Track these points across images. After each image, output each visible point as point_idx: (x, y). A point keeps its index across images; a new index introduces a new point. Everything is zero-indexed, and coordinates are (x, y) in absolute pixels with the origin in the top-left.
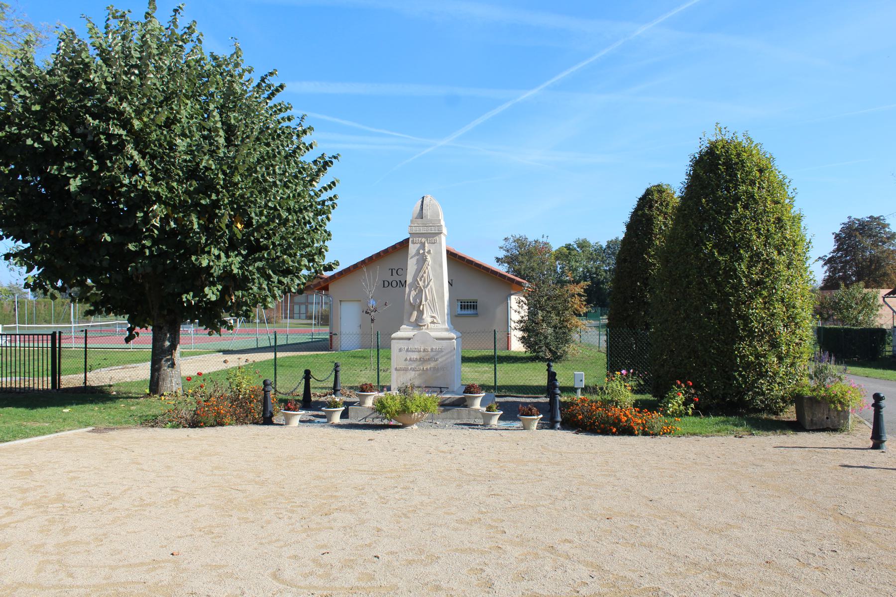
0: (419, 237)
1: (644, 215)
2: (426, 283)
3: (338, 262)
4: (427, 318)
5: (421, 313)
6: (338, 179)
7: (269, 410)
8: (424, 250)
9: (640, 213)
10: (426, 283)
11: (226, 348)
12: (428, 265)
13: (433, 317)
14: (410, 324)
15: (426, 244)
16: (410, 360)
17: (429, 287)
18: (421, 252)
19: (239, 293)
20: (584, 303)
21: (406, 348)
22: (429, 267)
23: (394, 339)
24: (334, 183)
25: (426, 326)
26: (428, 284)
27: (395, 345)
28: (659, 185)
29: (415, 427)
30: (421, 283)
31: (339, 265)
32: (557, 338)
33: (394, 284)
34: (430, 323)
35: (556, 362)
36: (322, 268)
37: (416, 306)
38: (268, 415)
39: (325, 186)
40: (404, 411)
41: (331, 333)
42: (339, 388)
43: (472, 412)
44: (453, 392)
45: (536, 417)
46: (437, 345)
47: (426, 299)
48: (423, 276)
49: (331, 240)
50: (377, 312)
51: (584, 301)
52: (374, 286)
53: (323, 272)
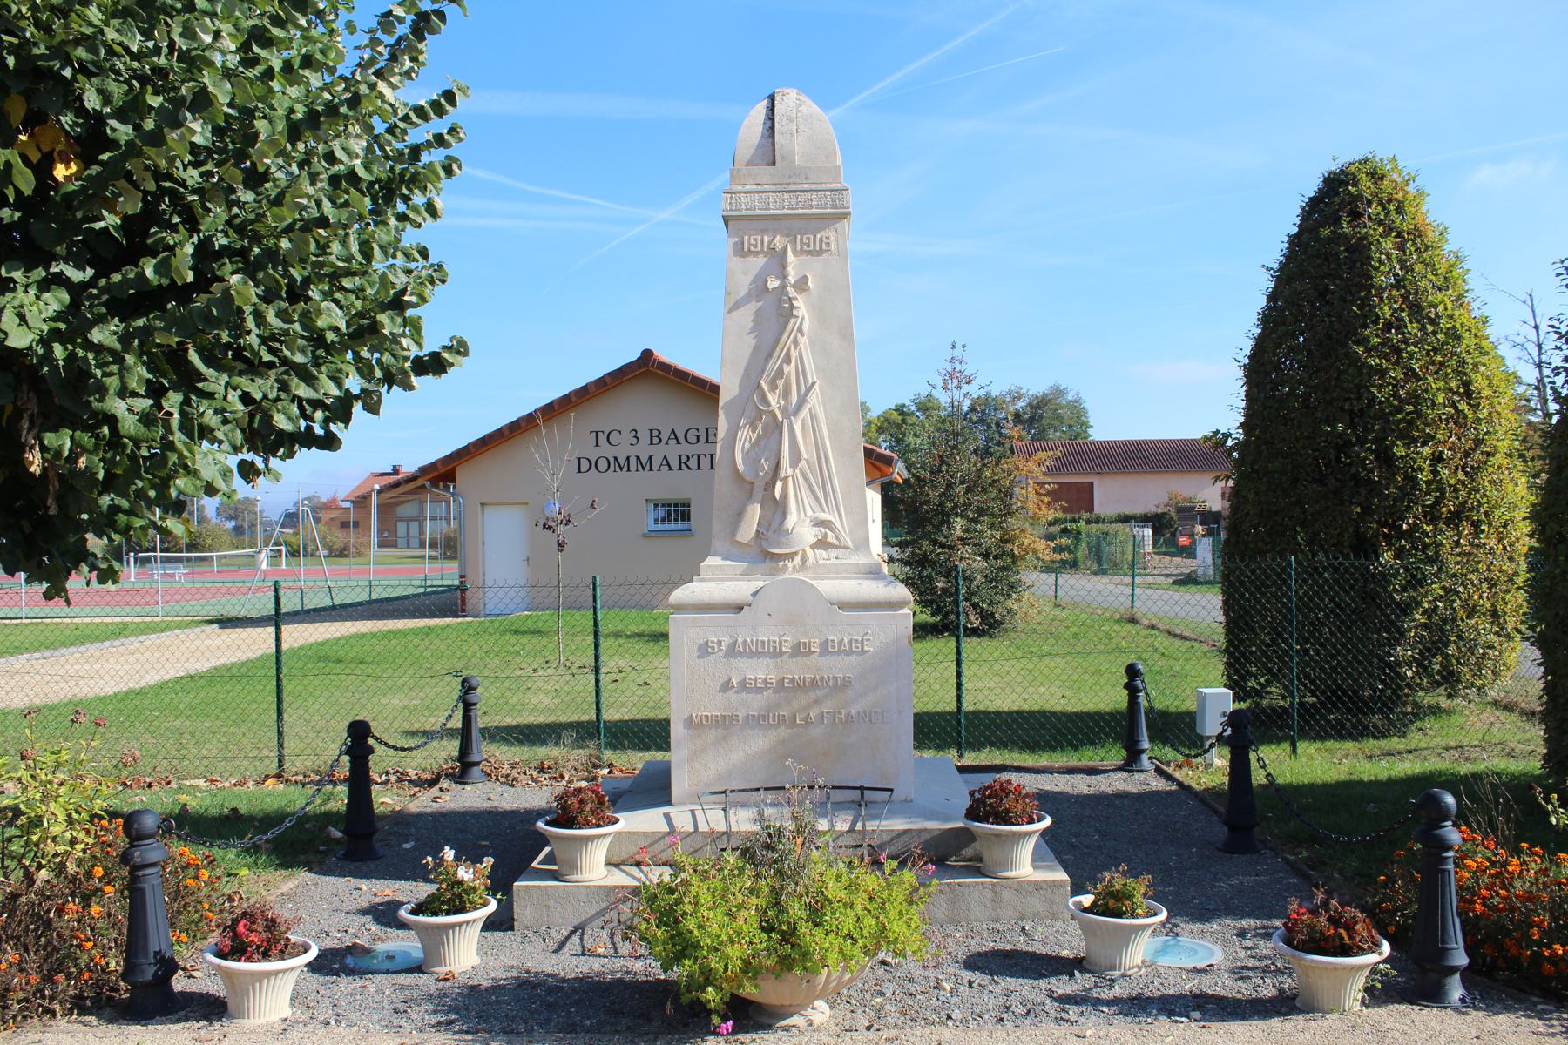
0: (763, 232)
1: (1337, 238)
2: (794, 399)
3: (462, 343)
4: (801, 525)
5: (777, 509)
6: (463, 84)
7: (154, 946)
8: (784, 277)
9: (1325, 232)
10: (794, 399)
11: (231, 611)
12: (800, 330)
13: (820, 523)
14: (736, 551)
15: (791, 257)
16: (744, 686)
17: (804, 413)
18: (773, 283)
19: (63, 440)
20: (1046, 499)
21: (726, 641)
22: (803, 340)
23: (680, 608)
24: (449, 96)
25: (798, 559)
26: (802, 401)
27: (685, 633)
28: (1366, 161)
29: (821, 1012)
30: (774, 400)
31: (466, 354)
32: (991, 582)
33: (602, 465)
34: (813, 547)
35: (991, 637)
36: (408, 364)
37: (759, 485)
38: (149, 972)
39: (422, 103)
40: (786, 963)
41: (462, 577)
42: (475, 758)
43: (1006, 894)
44: (906, 807)
45: (1372, 958)
46: (843, 629)
47: (796, 458)
48: (780, 373)
49: (443, 282)
50: (571, 525)
51: (1048, 494)
52: (562, 460)
53: (413, 379)
